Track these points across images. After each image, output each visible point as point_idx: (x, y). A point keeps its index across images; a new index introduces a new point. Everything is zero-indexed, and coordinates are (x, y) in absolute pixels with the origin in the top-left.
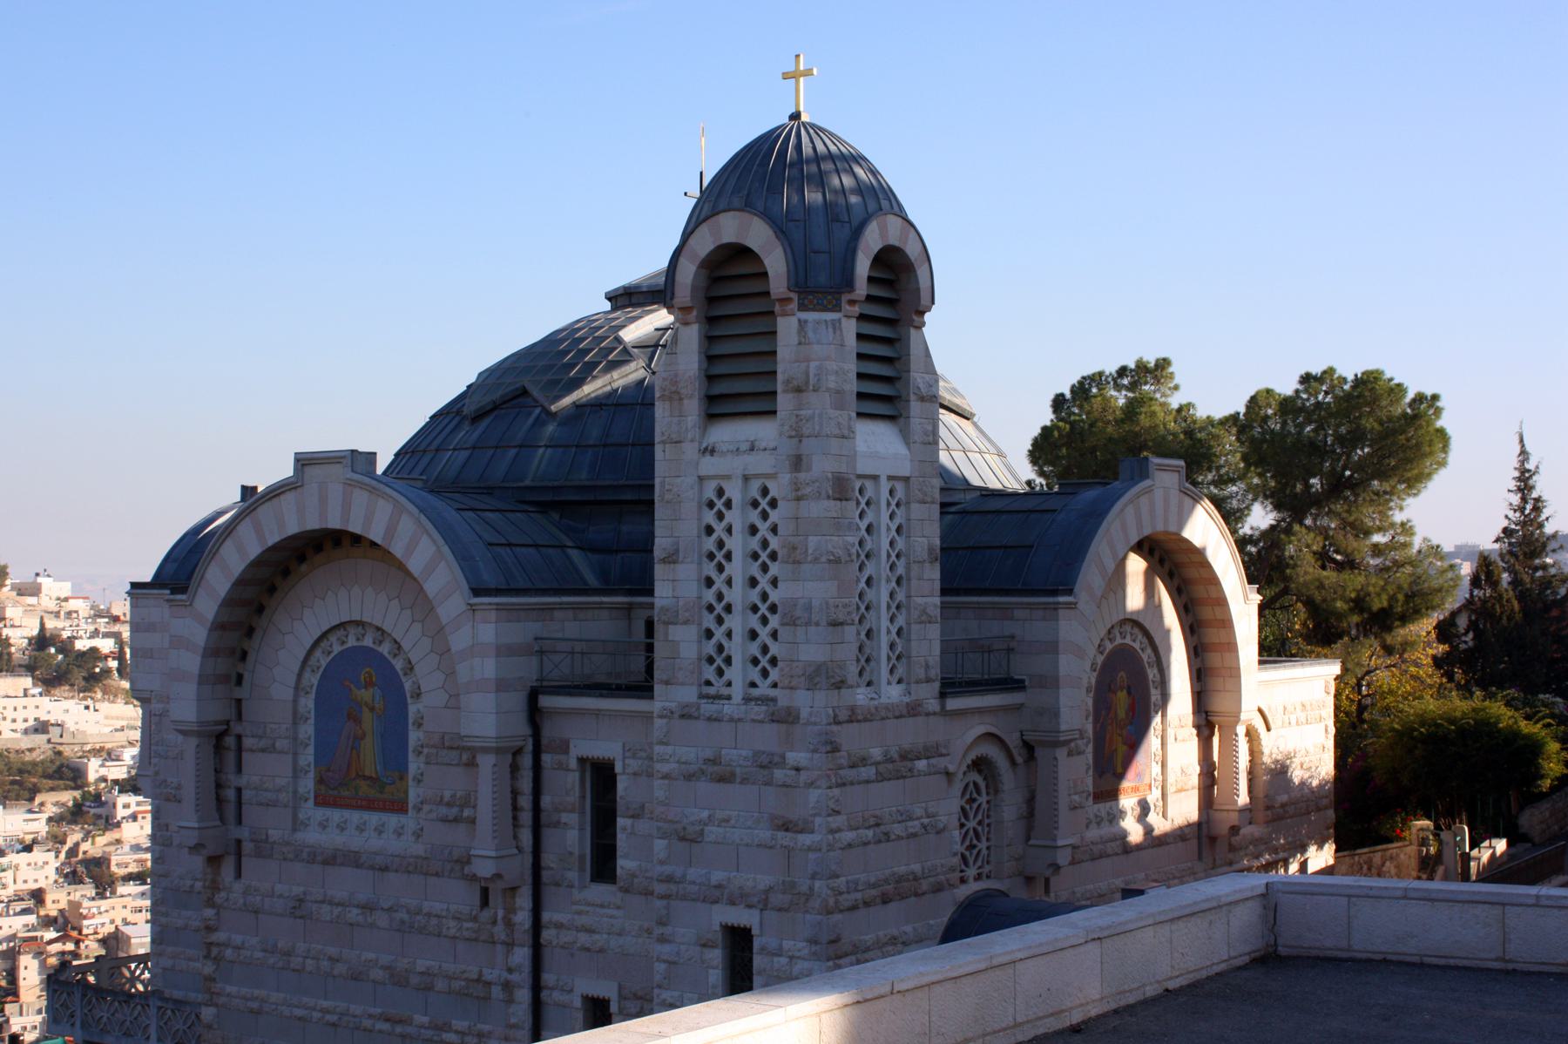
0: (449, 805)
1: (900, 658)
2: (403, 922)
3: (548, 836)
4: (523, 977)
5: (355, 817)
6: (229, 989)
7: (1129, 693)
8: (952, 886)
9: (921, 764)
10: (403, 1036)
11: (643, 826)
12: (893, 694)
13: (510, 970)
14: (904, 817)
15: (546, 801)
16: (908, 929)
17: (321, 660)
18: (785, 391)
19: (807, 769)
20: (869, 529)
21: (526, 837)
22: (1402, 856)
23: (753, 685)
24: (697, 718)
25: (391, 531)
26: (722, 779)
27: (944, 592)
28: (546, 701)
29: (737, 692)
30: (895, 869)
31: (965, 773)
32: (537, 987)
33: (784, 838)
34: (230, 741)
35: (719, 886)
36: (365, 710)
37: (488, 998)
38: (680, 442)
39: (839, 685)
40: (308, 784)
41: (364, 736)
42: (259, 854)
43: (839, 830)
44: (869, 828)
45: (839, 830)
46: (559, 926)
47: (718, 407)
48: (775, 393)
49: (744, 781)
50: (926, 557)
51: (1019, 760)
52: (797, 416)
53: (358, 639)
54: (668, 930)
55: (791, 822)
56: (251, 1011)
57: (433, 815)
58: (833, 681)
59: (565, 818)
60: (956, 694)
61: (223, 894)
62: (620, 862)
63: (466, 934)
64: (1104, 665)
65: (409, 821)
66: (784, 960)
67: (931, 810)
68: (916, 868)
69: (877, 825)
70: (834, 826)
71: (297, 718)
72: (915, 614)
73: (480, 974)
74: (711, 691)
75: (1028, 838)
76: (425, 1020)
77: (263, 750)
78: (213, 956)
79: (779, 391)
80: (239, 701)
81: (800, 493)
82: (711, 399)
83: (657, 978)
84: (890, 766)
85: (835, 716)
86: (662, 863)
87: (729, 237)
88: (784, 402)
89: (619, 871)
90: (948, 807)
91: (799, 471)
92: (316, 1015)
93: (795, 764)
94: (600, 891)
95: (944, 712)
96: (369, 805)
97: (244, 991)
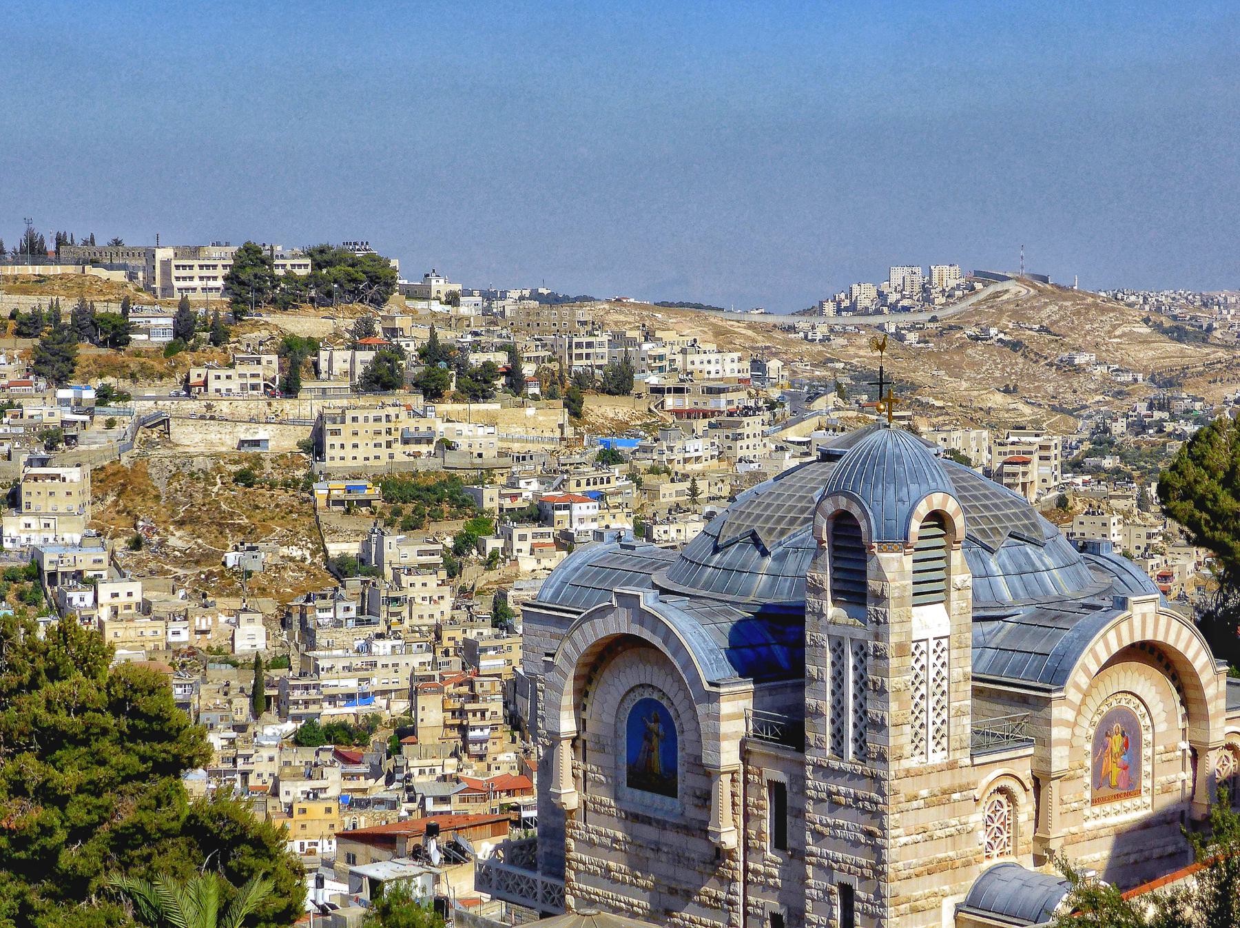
7: (1123, 735)
9: (956, 796)
12: (938, 758)
17: (629, 706)
31: (988, 798)
43: (898, 837)
50: (962, 679)
60: (979, 755)
65: (677, 802)
68: (951, 854)
80: (584, 721)
95: (974, 766)
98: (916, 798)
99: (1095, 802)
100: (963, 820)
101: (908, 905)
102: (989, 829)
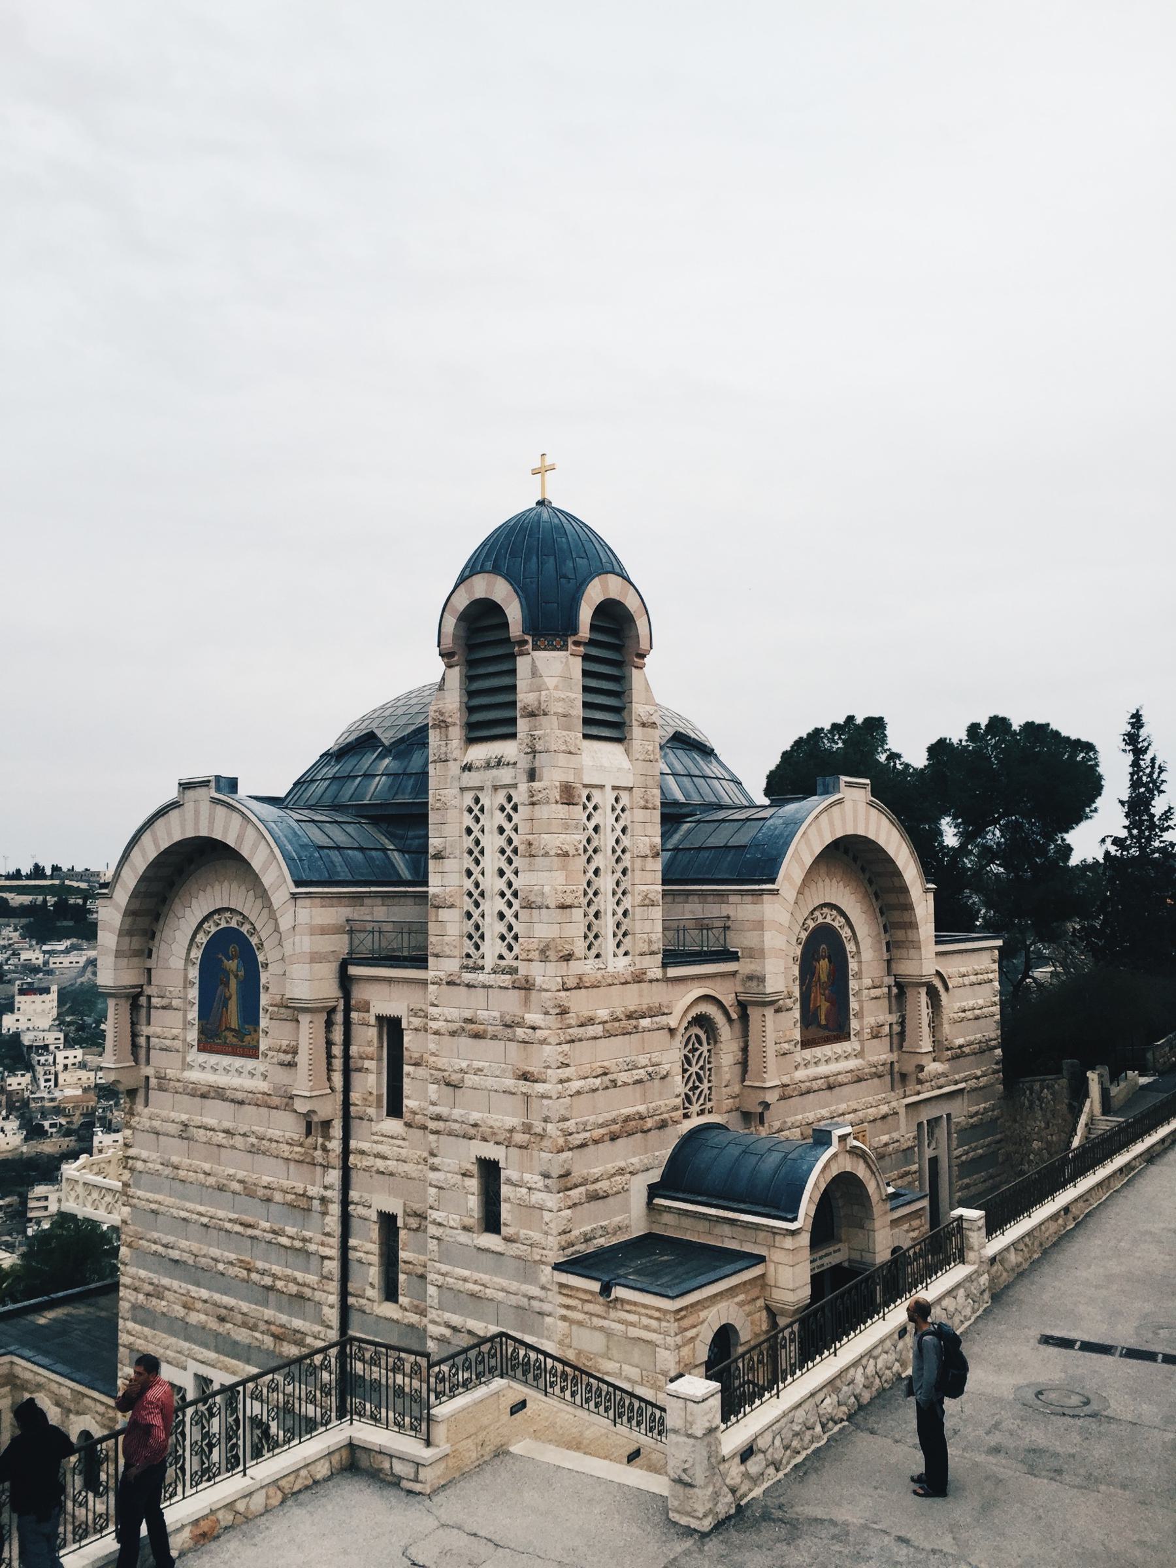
0: (285, 1052)
1: (622, 934)
2: (253, 1145)
3: (356, 1077)
4: (334, 1195)
5: (226, 1060)
6: (139, 1193)
7: (830, 961)
8: (677, 1122)
9: (645, 1022)
10: (252, 1238)
11: (421, 1072)
12: (619, 965)
13: (326, 1188)
14: (630, 1067)
15: (354, 1050)
16: (635, 1160)
17: (202, 939)
18: (522, 716)
19: (540, 1028)
20: (596, 829)
21: (338, 1079)
22: (1056, 1086)
23: (501, 957)
24: (459, 985)
25: (240, 838)
26: (477, 1036)
27: (664, 882)
28: (353, 970)
29: (489, 962)
30: (623, 1111)
31: (686, 1029)
32: (345, 1202)
33: (524, 1087)
34: (143, 1000)
35: (475, 1125)
36: (232, 977)
37: (310, 1210)
38: (448, 761)
39: (568, 958)
40: (193, 1035)
41: (230, 998)
42: (161, 1089)
43: (568, 1080)
44: (596, 1077)
45: (568, 1080)
46: (362, 1152)
47: (476, 733)
48: (516, 718)
49: (494, 1037)
51: (734, 1016)
52: (532, 735)
53: (227, 922)
54: (436, 1161)
55: (528, 1072)
56: (153, 1211)
57: (275, 1060)
58: (561, 954)
59: (367, 1064)
60: (676, 964)
61: (137, 1119)
62: (406, 1102)
63: (297, 1157)
64: (808, 938)
66: (524, 1190)
67: (654, 1060)
68: (642, 1108)
69: (605, 1074)
70: (563, 1076)
71: (187, 983)
72: (638, 899)
73: (305, 1191)
74: (470, 962)
75: (743, 1080)
76: (267, 1225)
77: (164, 1008)
78: (129, 1166)
79: (518, 716)
80: (149, 970)
81: (535, 799)
82: (470, 726)
83: (431, 1201)
84: (617, 1024)
85: (564, 984)
86: (434, 1104)
87: (480, 593)
88: (522, 725)
89: (405, 1109)
90: (671, 1056)
91: (534, 781)
92: (195, 1217)
93: (532, 1024)
94: (393, 1126)
96: (234, 1053)
97: (149, 1195)
98: (591, 1021)
99: (806, 1043)
100: (656, 1058)
101: (582, 1189)
102: (687, 1075)
